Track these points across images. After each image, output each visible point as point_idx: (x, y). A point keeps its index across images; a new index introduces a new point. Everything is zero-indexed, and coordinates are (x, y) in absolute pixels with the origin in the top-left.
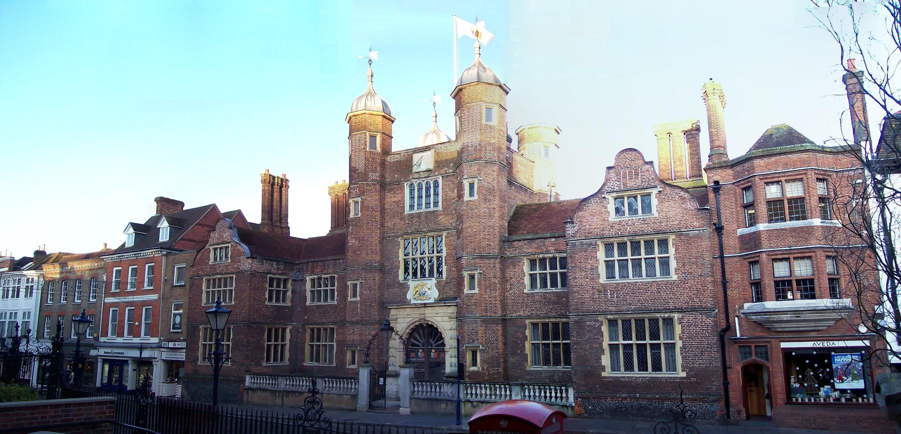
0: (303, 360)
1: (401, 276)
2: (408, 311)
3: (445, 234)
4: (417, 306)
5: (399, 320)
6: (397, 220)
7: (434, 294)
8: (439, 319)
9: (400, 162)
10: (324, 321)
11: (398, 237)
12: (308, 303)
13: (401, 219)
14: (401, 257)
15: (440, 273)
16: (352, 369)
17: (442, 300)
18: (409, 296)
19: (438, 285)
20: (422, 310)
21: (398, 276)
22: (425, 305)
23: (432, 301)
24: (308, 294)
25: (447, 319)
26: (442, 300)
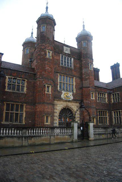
0: (2, 120)
1: (59, 89)
2: (62, 102)
3: (75, 78)
4: (66, 101)
5: (58, 105)
6: (57, 66)
7: (72, 98)
8: (73, 107)
9: (58, 46)
10: (17, 100)
11: (58, 73)
12: (6, 90)
13: (59, 66)
14: (59, 81)
15: (73, 91)
16: (48, 125)
17: (74, 100)
18: (62, 96)
19: (73, 95)
20: (67, 103)
21: (57, 88)
22: (69, 101)
23: (71, 100)
24: (7, 85)
25: (76, 107)
26: (74, 100)
